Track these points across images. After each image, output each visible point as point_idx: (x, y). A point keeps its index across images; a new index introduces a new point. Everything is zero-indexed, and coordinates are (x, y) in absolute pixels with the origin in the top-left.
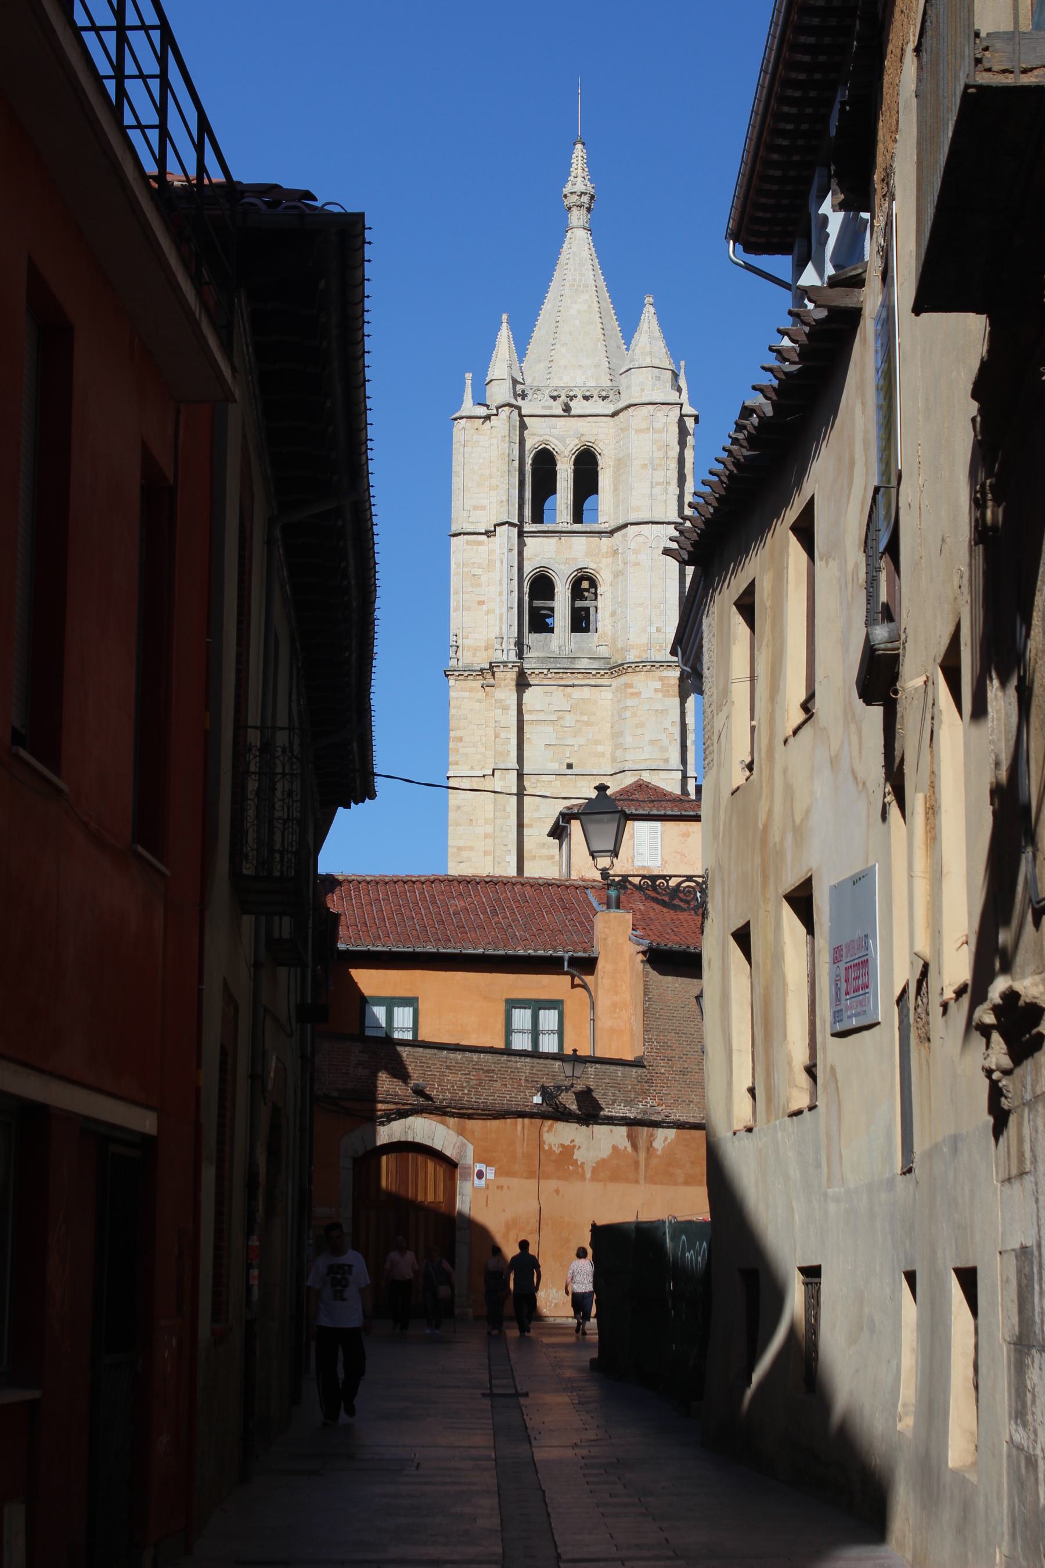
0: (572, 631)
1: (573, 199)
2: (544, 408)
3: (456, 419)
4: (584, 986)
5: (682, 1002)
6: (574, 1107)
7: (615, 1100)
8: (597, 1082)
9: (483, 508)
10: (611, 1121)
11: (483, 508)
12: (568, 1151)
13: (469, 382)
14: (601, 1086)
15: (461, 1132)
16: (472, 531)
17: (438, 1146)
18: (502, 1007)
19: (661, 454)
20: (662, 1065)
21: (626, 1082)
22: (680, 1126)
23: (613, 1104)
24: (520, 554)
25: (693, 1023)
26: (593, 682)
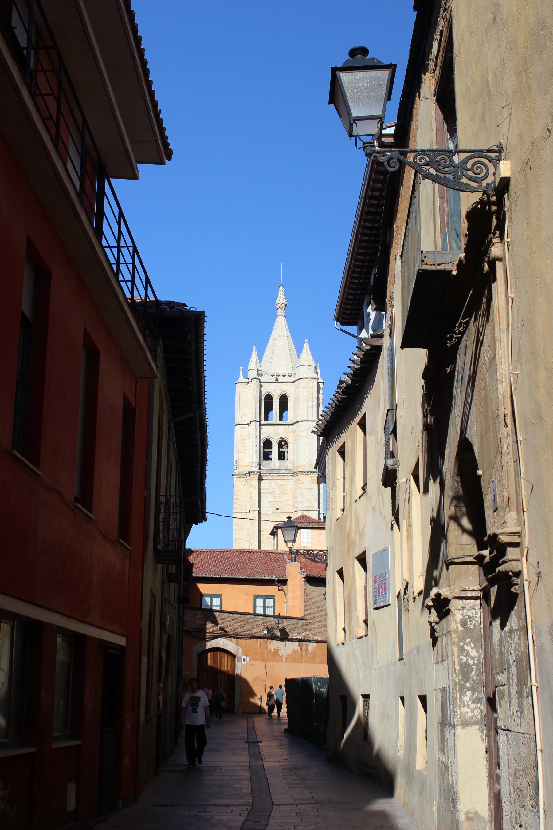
0: (279, 460)
1: (279, 306)
2: (268, 379)
3: (237, 383)
4: (283, 590)
6: (279, 635)
9: (246, 415)
10: (292, 640)
11: (246, 415)
12: (276, 651)
13: (241, 370)
15: (237, 644)
16: (242, 424)
17: (229, 649)
18: (253, 598)
19: (311, 396)
22: (318, 642)
23: (293, 634)
24: (260, 432)
26: (286, 478)
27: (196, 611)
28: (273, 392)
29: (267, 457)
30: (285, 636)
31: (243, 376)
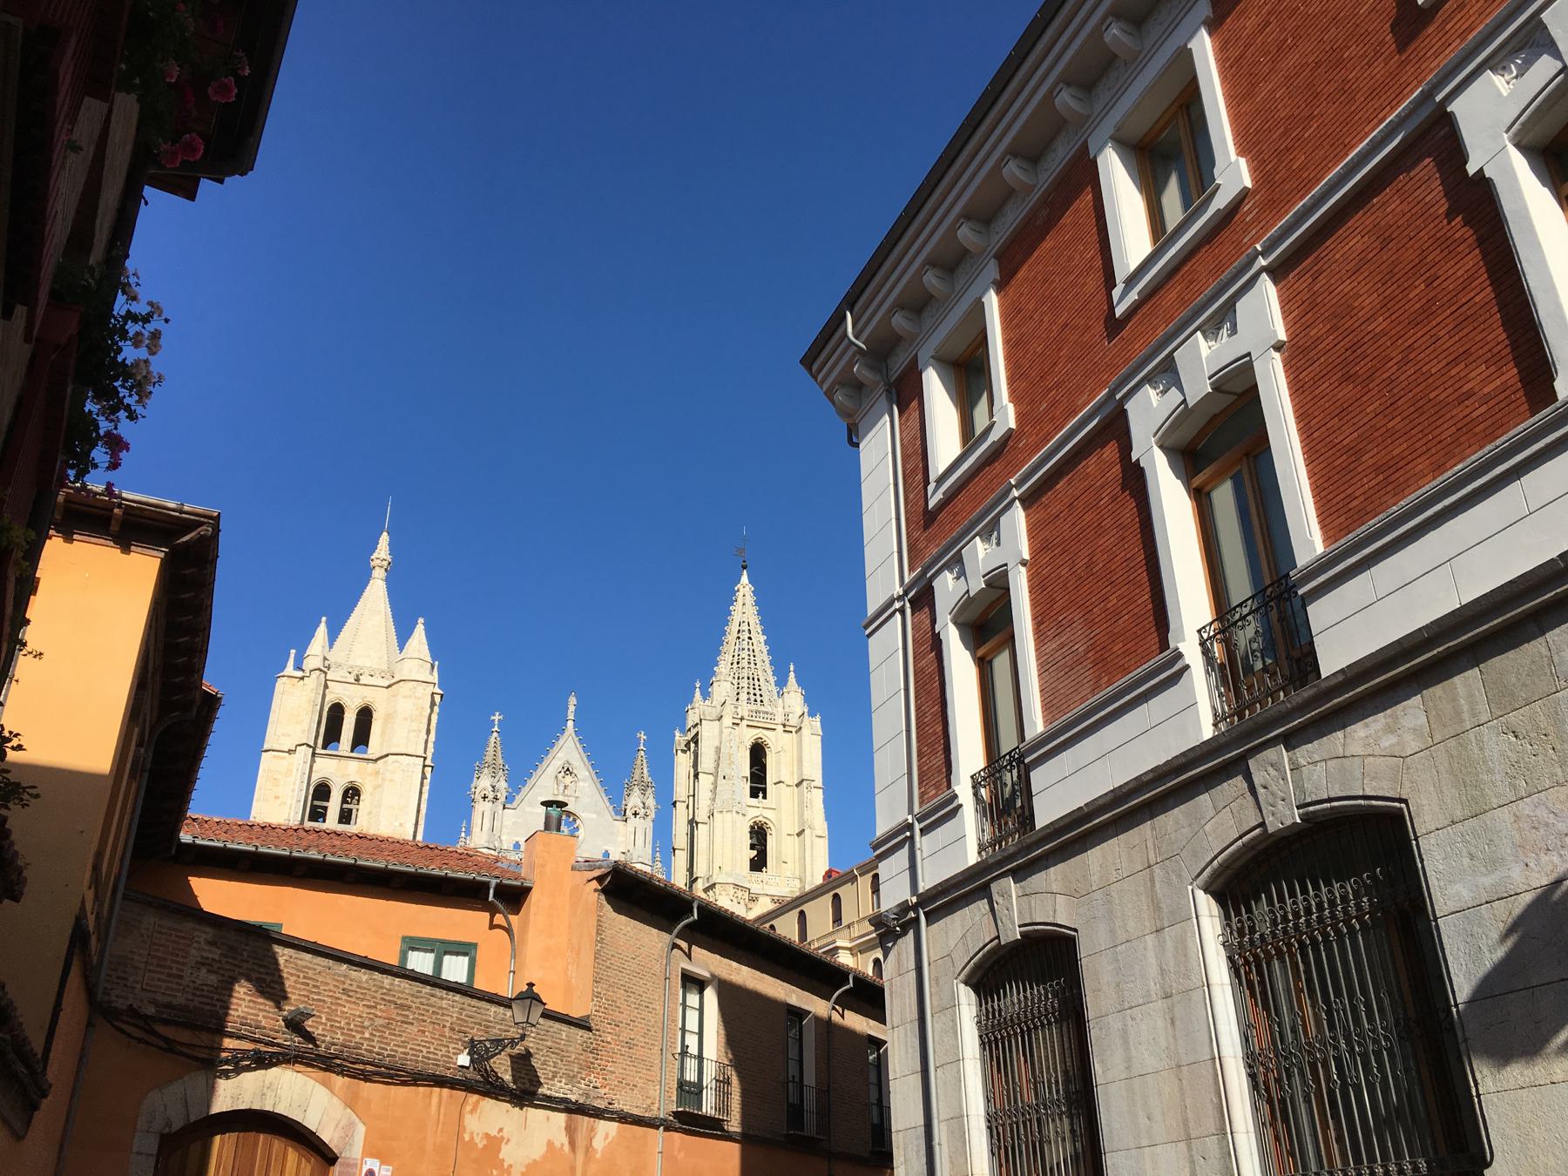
1: (378, 562)
4: (508, 930)
5: (634, 951)
6: (507, 1077)
7: (556, 1072)
8: (539, 1044)
9: (289, 735)
11: (289, 735)
12: (494, 1143)
14: (542, 1050)
15: (351, 1102)
17: (311, 1122)
20: (609, 1031)
21: (570, 1049)
22: (624, 1118)
23: (554, 1077)
25: (642, 981)
27: (189, 925)
28: (347, 699)
29: (317, 814)
30: (528, 1085)
31: (294, 666)
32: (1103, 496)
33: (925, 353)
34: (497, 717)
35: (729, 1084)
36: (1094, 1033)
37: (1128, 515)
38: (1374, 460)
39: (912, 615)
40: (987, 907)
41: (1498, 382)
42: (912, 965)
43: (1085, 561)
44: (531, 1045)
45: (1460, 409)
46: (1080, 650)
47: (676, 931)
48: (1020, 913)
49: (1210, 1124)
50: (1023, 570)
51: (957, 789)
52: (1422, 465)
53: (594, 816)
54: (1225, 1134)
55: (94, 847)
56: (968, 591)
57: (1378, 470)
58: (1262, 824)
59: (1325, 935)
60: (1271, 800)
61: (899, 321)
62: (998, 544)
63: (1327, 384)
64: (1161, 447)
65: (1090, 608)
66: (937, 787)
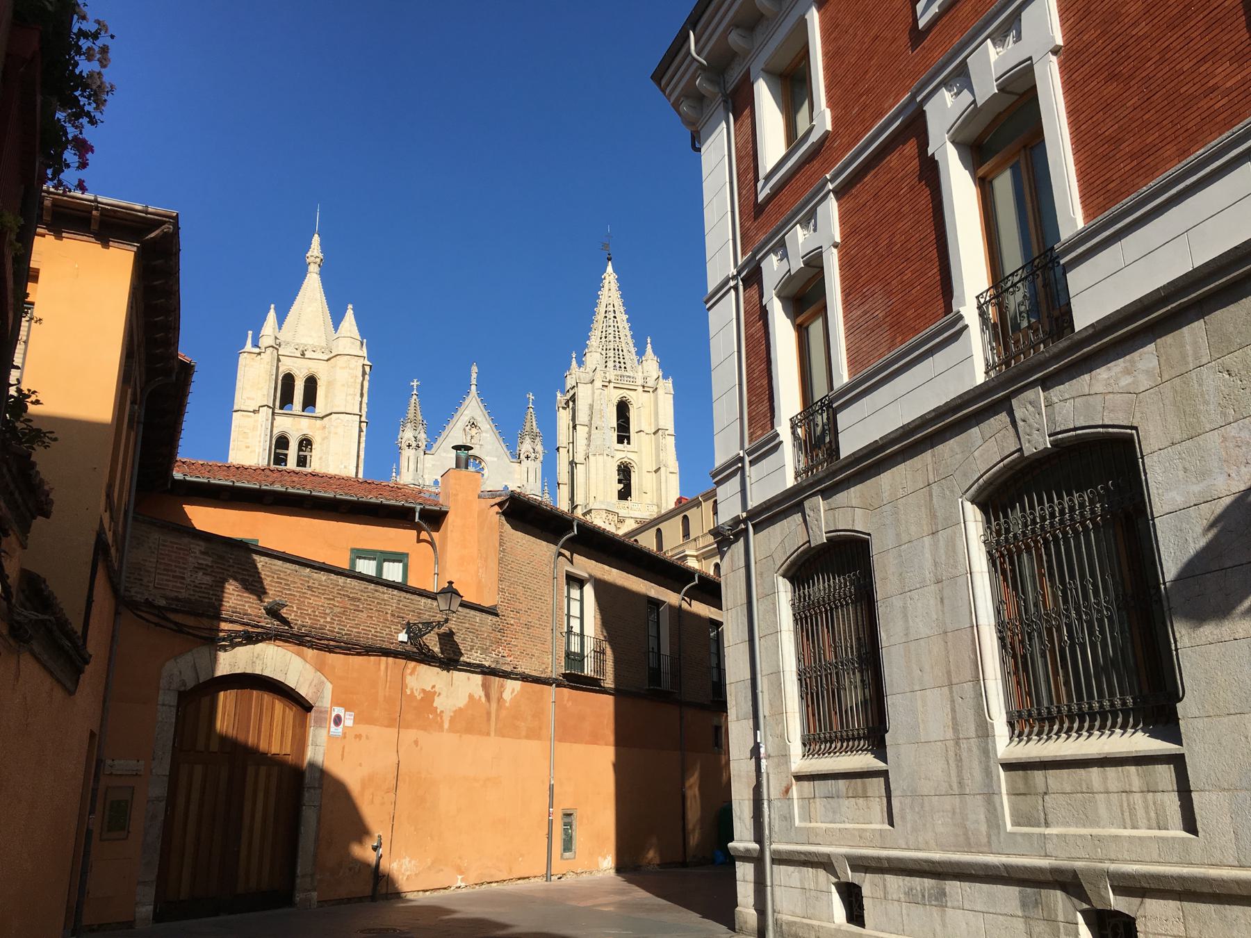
4: (432, 544)
6: (437, 649)
9: (253, 399)
11: (253, 399)
12: (429, 696)
14: (461, 630)
15: (320, 668)
17: (291, 682)
18: (348, 555)
19: (352, 380)
22: (525, 678)
23: (472, 649)
27: (186, 540)
29: (280, 459)
30: (452, 655)
31: (252, 343)
32: (903, 186)
33: (757, 65)
34: (415, 383)
35: (604, 654)
36: (882, 610)
37: (923, 202)
38: (1130, 148)
39: (744, 291)
40: (801, 519)
41: (1239, 77)
42: (742, 563)
43: (886, 242)
44: (453, 626)
45: (1205, 100)
46: (880, 315)
47: (561, 543)
48: (826, 523)
49: (968, 673)
50: (835, 251)
51: (779, 429)
52: (1170, 150)
53: (496, 459)
54: (979, 680)
55: (105, 479)
56: (789, 270)
57: (1133, 156)
58: (1020, 450)
59: (1065, 533)
60: (1028, 430)
61: (735, 39)
62: (815, 230)
63: (1095, 83)
64: (953, 142)
65: (889, 281)
66: (763, 428)
